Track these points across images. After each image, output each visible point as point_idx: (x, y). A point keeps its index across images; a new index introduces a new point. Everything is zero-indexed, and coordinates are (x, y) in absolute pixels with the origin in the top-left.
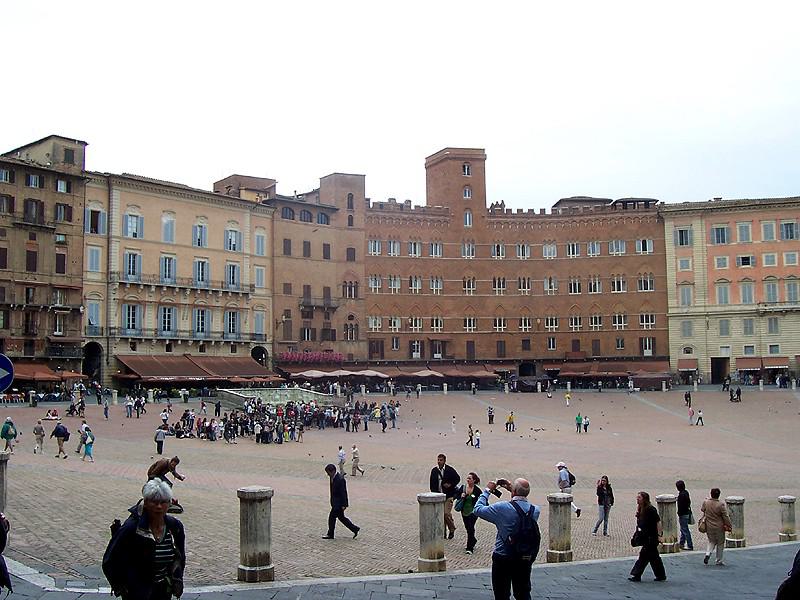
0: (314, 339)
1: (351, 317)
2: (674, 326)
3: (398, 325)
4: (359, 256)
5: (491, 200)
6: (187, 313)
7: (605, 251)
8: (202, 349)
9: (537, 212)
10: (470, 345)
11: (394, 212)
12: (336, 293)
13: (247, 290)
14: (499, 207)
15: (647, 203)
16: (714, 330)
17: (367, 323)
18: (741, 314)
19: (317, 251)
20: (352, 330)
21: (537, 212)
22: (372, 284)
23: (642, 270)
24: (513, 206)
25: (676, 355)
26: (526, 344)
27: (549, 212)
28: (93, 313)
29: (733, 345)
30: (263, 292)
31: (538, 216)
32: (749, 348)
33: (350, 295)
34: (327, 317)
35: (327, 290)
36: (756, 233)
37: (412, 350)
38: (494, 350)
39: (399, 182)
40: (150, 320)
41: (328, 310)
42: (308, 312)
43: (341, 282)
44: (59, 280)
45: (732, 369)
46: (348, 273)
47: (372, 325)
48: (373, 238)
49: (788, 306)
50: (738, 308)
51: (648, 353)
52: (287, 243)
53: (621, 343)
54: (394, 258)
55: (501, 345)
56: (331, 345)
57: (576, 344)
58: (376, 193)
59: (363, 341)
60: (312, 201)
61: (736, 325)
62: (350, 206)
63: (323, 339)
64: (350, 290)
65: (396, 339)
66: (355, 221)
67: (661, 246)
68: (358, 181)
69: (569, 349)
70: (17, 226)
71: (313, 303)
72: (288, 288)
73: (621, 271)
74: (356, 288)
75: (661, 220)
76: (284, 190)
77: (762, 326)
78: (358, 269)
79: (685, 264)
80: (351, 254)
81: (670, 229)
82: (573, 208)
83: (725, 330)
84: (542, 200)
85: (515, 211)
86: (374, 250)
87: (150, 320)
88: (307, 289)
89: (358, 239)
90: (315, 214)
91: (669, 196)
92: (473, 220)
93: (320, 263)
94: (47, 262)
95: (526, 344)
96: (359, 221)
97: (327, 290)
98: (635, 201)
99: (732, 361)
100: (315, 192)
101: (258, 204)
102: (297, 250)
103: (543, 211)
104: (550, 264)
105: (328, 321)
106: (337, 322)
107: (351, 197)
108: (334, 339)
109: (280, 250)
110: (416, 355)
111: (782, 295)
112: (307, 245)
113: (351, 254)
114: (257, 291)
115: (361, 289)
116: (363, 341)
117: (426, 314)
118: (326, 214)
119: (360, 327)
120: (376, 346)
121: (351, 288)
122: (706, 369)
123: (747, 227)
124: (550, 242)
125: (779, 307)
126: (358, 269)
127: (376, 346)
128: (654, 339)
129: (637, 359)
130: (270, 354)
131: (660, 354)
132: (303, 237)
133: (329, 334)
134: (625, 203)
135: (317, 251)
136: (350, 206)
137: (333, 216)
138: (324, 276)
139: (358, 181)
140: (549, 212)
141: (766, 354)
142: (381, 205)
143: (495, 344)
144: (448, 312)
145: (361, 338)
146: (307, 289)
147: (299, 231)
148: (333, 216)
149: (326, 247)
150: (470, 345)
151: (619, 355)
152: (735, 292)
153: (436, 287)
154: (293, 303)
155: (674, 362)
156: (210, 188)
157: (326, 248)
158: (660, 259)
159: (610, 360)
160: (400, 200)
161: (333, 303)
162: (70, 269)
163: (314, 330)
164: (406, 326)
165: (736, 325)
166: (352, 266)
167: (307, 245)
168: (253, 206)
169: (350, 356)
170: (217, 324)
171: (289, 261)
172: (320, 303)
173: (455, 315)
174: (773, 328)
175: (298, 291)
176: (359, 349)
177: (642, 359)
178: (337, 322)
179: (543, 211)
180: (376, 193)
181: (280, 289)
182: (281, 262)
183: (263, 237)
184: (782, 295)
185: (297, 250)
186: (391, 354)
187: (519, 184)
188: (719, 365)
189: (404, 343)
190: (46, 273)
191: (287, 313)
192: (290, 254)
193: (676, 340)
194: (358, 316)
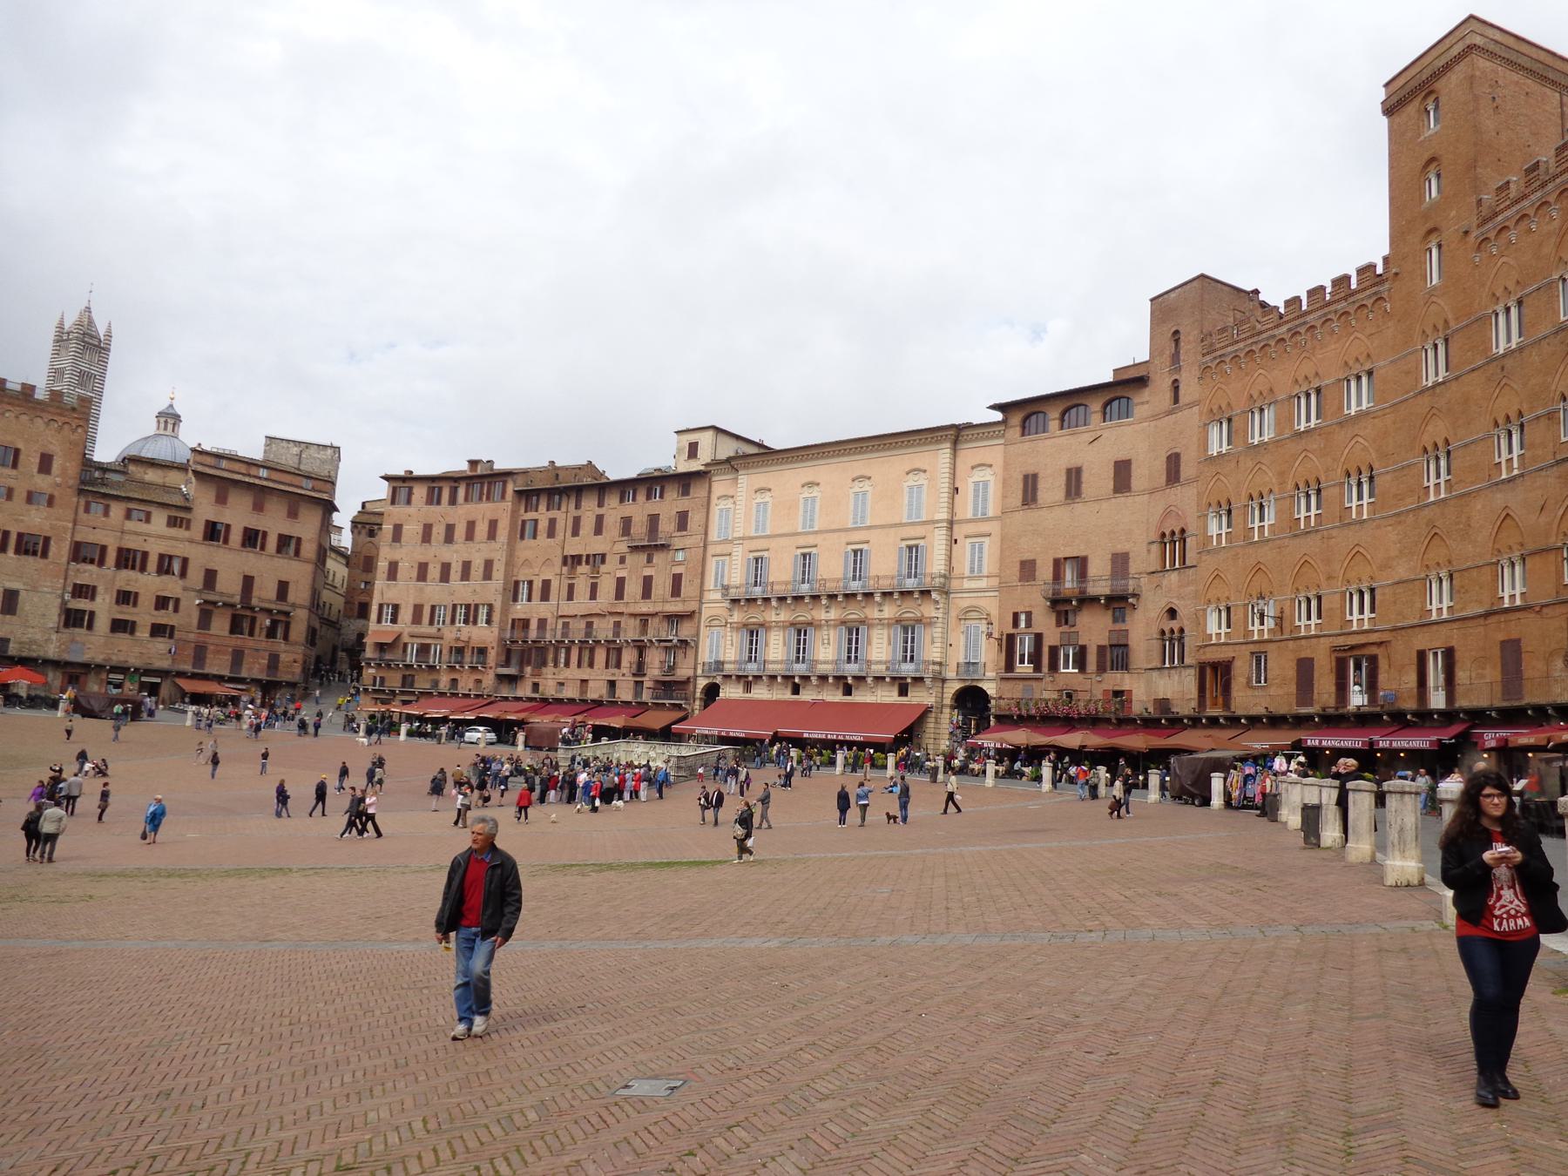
6: (833, 634)
8: (848, 691)
17: (1200, 621)
20: (1172, 641)
28: (719, 646)
30: (983, 584)
35: (1120, 562)
38: (1493, 673)
40: (776, 649)
43: (1155, 536)
44: (675, 607)
46: (1167, 513)
52: (1030, 486)
59: (1190, 666)
63: (1101, 669)
70: (635, 549)
87: (776, 649)
93: (1105, 505)
94: (662, 587)
97: (1120, 562)
102: (1052, 489)
105: (1119, 626)
106: (1142, 629)
116: (1190, 666)
126: (1185, 498)
132: (1066, 461)
135: (1098, 479)
138: (1110, 530)
143: (1497, 651)
144: (1385, 566)
145: (1187, 661)
154: (1035, 599)
162: (686, 589)
163: (1083, 649)
170: (880, 649)
171: (1032, 515)
175: (1045, 572)
182: (1022, 517)
183: (986, 483)
185: (1052, 489)
189: (1282, 667)
190: (661, 601)
192: (1034, 499)
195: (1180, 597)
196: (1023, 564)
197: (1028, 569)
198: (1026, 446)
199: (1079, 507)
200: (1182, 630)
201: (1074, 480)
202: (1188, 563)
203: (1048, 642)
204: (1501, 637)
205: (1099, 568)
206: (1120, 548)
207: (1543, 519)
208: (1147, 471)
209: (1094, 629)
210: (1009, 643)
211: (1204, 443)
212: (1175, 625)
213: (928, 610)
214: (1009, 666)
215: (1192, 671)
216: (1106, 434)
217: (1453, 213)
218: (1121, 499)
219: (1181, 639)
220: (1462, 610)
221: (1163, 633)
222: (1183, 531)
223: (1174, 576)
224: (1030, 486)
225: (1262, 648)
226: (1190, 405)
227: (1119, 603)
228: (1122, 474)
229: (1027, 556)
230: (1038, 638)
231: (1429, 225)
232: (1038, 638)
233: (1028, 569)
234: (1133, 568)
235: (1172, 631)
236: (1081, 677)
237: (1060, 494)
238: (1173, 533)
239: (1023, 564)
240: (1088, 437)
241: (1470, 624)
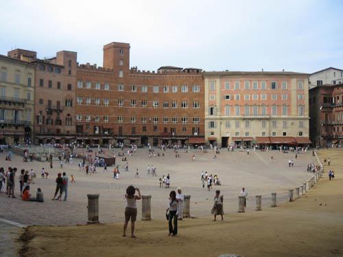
0: (52, 124)
1: (69, 115)
2: (207, 123)
3: (89, 119)
4: (73, 88)
5: (132, 65)
7: (179, 90)
9: (151, 72)
10: (120, 129)
11: (88, 69)
12: (62, 104)
13: (23, 101)
14: (134, 70)
15: (198, 71)
16: (223, 126)
17: (75, 118)
18: (234, 119)
19: (54, 85)
21: (151, 72)
22: (78, 101)
23: (195, 99)
24: (141, 69)
25: (207, 136)
26: (144, 129)
27: (156, 72)
29: (230, 132)
31: (151, 74)
32: (237, 133)
34: (58, 114)
36: (242, 86)
37: (95, 129)
39: (92, 56)
41: (59, 111)
42: (50, 112)
45: (230, 142)
47: (78, 118)
48: (80, 80)
49: (253, 117)
50: (233, 117)
51: (196, 134)
52: (42, 81)
53: (184, 129)
54: (88, 90)
55: (134, 129)
56: (60, 127)
57: (166, 129)
58: (81, 60)
60: (53, 62)
61: (233, 123)
62: (70, 65)
63: (56, 124)
65: (88, 124)
67: (203, 89)
68: (74, 55)
69: (163, 131)
71: (52, 108)
72: (41, 101)
73: (186, 99)
75: (203, 78)
76: (40, 56)
77: (243, 124)
78: (72, 94)
79: (212, 97)
80: (69, 87)
81: (206, 80)
82: (166, 70)
83: (228, 125)
84: (153, 67)
85: (141, 71)
86: (80, 85)
88: (50, 102)
89: (72, 80)
90: (54, 69)
91: (207, 68)
92: (124, 74)
95: (144, 129)
96: (74, 72)
98: (193, 70)
99: (230, 139)
100: (55, 58)
101: (29, 63)
102: (46, 84)
103: (154, 72)
104: (156, 95)
107: (70, 61)
108: (61, 124)
109: (38, 84)
110: (97, 132)
111: (251, 112)
112: (50, 82)
113: (69, 87)
114: (28, 102)
115: (74, 102)
117: (102, 114)
118: (60, 68)
119: (73, 119)
120: (79, 128)
121: (69, 102)
122: (219, 141)
123: (238, 84)
124: (156, 85)
125: (249, 117)
126: (72, 94)
127: (79, 128)
128: (199, 129)
129: (191, 137)
130: (33, 130)
131: (201, 135)
133: (59, 122)
134: (189, 70)
135: (54, 85)
136: (70, 65)
137: (62, 70)
138: (57, 96)
139: (74, 55)
140: (156, 72)
141: (244, 136)
142: (83, 66)
146: (50, 102)
147: (47, 76)
148: (62, 70)
149: (59, 84)
150: (120, 129)
151: (183, 134)
152: (232, 110)
153: (107, 103)
154: (43, 108)
155: (206, 138)
156: (6, 55)
157: (59, 84)
158: (202, 95)
159: (180, 136)
160: (92, 64)
161: (61, 109)
163: (52, 120)
164: (93, 119)
165: (233, 123)
166: (69, 92)
167: (50, 82)
168: (27, 65)
169: (68, 132)
172: (55, 108)
173: (114, 116)
174: (247, 126)
175: (46, 103)
176: (72, 129)
177: (193, 137)
178: (63, 117)
179: (154, 72)
180: (81, 60)
181: (38, 101)
184: (251, 112)
185: (46, 84)
186: (85, 131)
187: (143, 60)
188: (225, 140)
189: (91, 127)
191: (41, 112)
193: (207, 130)
194: (72, 115)
200: (71, 119)
203: (46, 118)
208: (64, 85)
209: (54, 117)
210: (37, 117)
211: (76, 85)
213: (21, 107)
214: (38, 123)
218: (58, 90)
230: (44, 117)
232: (44, 117)
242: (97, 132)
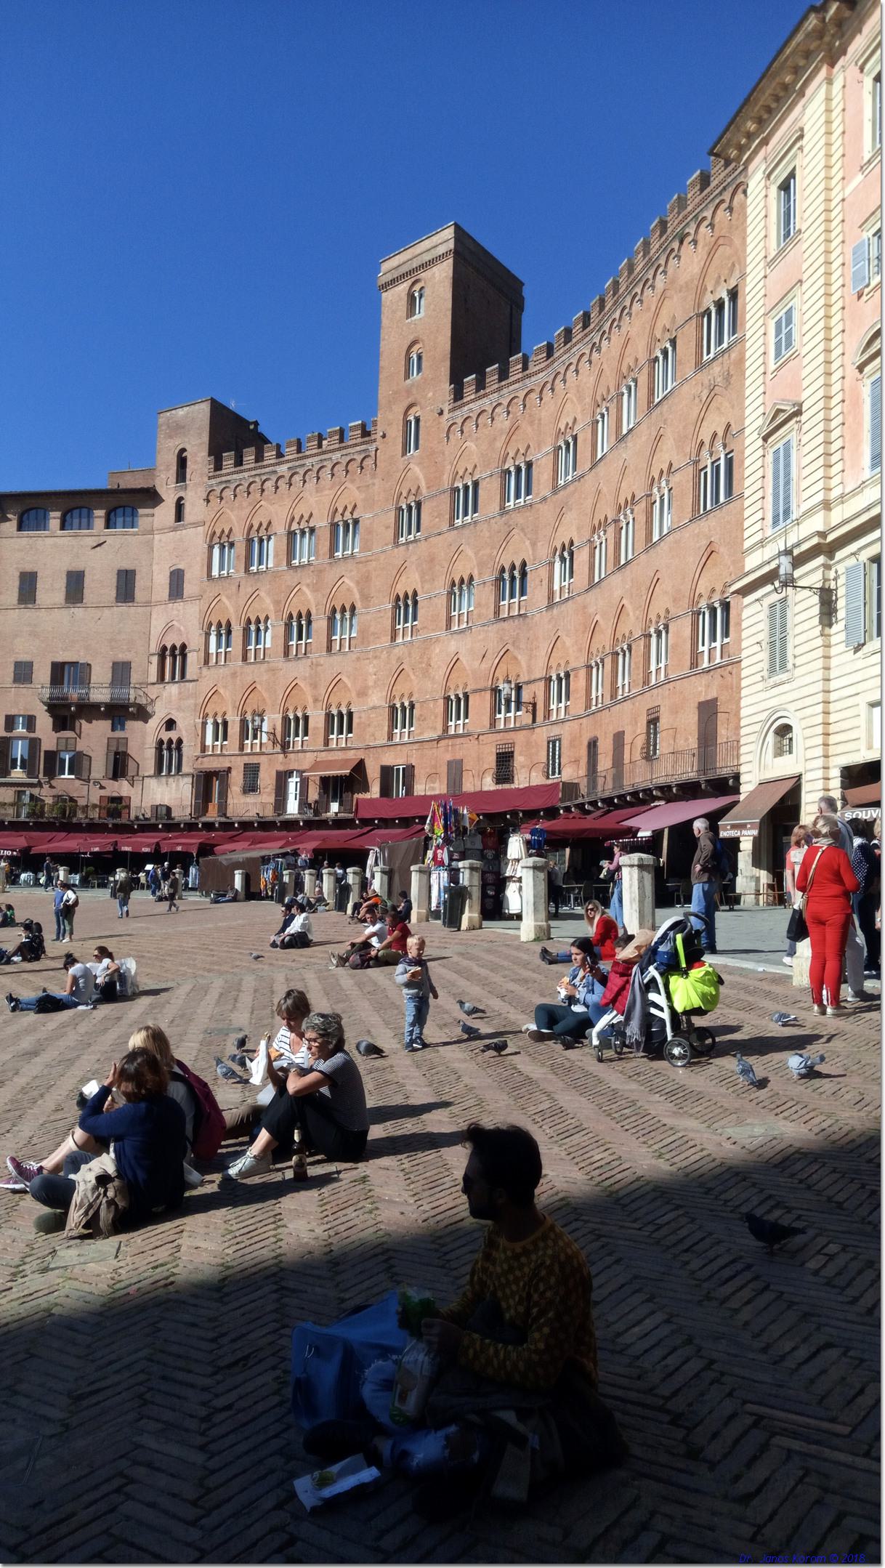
19: (100, 585)
20: (168, 755)
33: (173, 677)
35: (121, 671)
42: (64, 715)
52: (28, 587)
56: (122, 788)
59: (187, 775)
62: (181, 476)
64: (174, 657)
66: (188, 510)
74: (184, 656)
93: (107, 611)
97: (121, 671)
102: (51, 590)
105: (119, 734)
116: (187, 775)
135: (100, 585)
136: (181, 476)
145: (185, 769)
171: (28, 614)
175: (42, 675)
185: (51, 590)
195: (179, 709)
196: (18, 665)
197: (23, 673)
198: (24, 541)
199: (78, 612)
200: (180, 741)
201: (75, 585)
202: (188, 677)
204: (449, 757)
205: (101, 675)
206: (122, 657)
207: (484, 666)
209: (94, 737)
212: (173, 735)
215: (189, 780)
216: (110, 540)
217: (430, 394)
218: (124, 608)
219: (179, 748)
220: (421, 734)
221: (161, 742)
222: (184, 647)
223: (173, 689)
224: (28, 587)
225: (254, 760)
226: (196, 525)
227: (121, 713)
228: (126, 585)
229: (24, 657)
231: (410, 400)
233: (23, 673)
234: (135, 677)
235: (170, 741)
236: (78, 782)
237: (60, 596)
238: (174, 647)
239: (18, 665)
240: (92, 541)
241: (426, 745)
242: (292, 807)
